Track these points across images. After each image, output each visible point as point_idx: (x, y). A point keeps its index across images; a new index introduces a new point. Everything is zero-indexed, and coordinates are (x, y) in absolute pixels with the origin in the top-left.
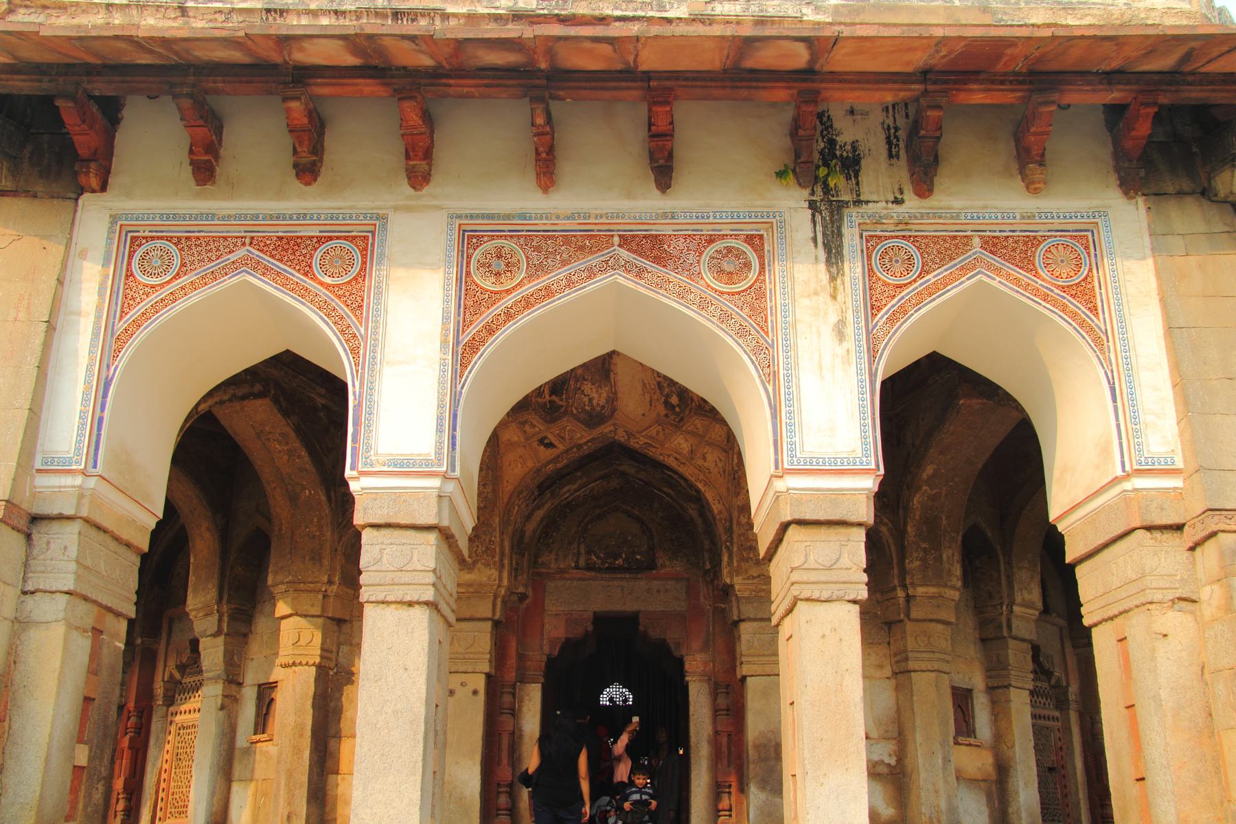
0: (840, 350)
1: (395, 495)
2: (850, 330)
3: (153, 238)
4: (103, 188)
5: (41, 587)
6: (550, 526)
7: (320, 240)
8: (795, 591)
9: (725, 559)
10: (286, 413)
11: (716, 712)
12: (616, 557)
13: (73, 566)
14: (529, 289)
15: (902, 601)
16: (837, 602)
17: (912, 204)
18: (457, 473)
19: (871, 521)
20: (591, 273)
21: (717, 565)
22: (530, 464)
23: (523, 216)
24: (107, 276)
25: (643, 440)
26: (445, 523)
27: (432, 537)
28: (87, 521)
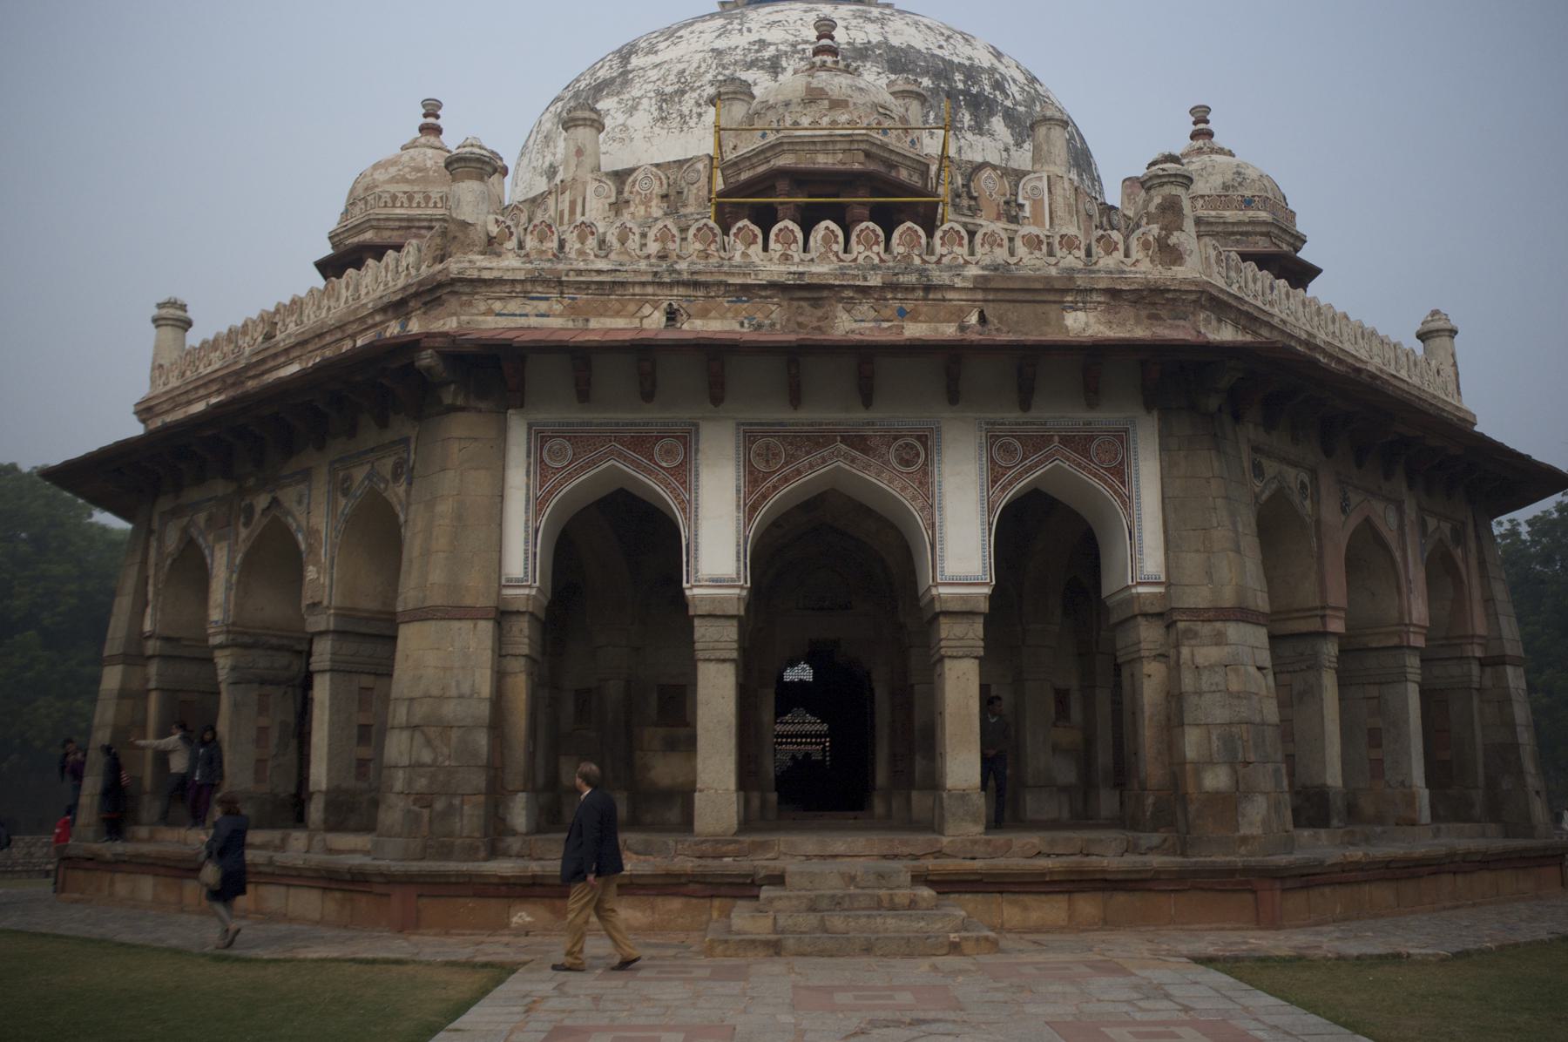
1: (713, 599)
4: (522, 406)
5: (510, 652)
7: (658, 438)
8: (943, 652)
13: (526, 640)
14: (787, 470)
16: (965, 660)
17: (1014, 415)
18: (749, 585)
19: (987, 611)
20: (824, 461)
23: (781, 424)
24: (529, 464)
28: (532, 614)
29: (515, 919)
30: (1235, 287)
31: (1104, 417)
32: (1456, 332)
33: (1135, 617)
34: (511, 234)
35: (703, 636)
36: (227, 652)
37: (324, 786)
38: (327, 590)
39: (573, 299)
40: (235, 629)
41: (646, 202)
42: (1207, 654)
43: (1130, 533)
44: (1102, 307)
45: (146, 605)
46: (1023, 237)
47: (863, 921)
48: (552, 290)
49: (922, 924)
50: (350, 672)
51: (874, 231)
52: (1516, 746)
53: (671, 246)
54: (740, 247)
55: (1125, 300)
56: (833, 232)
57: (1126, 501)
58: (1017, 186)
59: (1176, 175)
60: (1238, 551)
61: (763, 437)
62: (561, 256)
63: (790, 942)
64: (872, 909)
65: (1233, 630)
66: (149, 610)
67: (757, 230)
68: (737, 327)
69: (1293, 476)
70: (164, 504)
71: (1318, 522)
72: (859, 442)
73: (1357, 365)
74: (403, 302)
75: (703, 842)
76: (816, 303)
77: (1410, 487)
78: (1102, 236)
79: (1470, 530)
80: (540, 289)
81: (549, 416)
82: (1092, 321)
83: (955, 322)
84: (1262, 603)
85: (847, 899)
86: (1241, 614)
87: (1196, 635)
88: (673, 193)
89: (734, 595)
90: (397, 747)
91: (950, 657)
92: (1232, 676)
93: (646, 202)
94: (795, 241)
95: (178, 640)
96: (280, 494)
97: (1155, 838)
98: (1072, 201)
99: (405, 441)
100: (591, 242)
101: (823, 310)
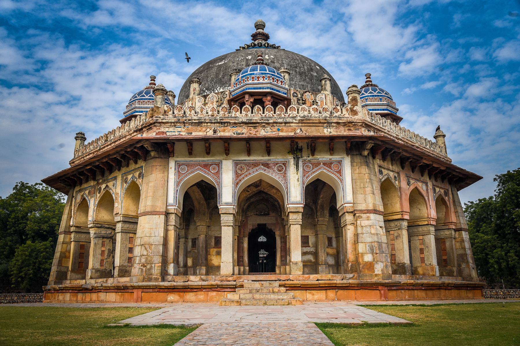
0: (298, 183)
1: (226, 209)
2: (300, 180)
3: (182, 165)
4: (173, 157)
6: (249, 206)
7: (211, 165)
8: (290, 223)
9: (283, 213)
10: (198, 188)
11: (281, 242)
12: (262, 212)
13: (174, 221)
15: (317, 221)
17: (311, 157)
18: (236, 205)
19: (303, 211)
21: (281, 214)
22: (245, 195)
23: (245, 161)
25: (266, 190)
26: (234, 213)
27: (232, 215)
29: (169, 299)
30: (374, 121)
31: (335, 158)
32: (445, 136)
33: (345, 213)
34: (171, 110)
35: (223, 219)
36: (93, 229)
37: (118, 265)
38: (120, 209)
40: (95, 222)
41: (212, 103)
42: (365, 223)
43: (343, 189)
44: (335, 127)
45: (71, 217)
46: (313, 108)
47: (264, 296)
48: (182, 125)
49: (281, 296)
50: (127, 233)
51: (271, 108)
52: (466, 255)
53: (215, 112)
54: (234, 112)
56: (259, 108)
57: (342, 181)
58: (316, 97)
59: (355, 91)
60: (374, 194)
61: (240, 164)
62: (185, 115)
63: (243, 302)
64: (267, 293)
65: (372, 216)
66: (72, 219)
67: (239, 108)
68: (233, 134)
69: (391, 174)
70: (77, 188)
71: (400, 188)
72: (266, 165)
74: (142, 129)
75: (222, 277)
76: (255, 127)
77: (430, 179)
78: (335, 108)
79: (450, 192)
80: (178, 125)
81: (180, 159)
83: (293, 132)
84: (381, 209)
85: (260, 290)
86: (375, 211)
87: (361, 217)
88: (219, 100)
89: (232, 209)
90: (137, 251)
91: (292, 224)
93: (212, 103)
94: (249, 110)
95: (80, 227)
96: (108, 184)
97: (351, 275)
98: (332, 101)
99: (142, 167)
100: (193, 112)
101: (257, 129)
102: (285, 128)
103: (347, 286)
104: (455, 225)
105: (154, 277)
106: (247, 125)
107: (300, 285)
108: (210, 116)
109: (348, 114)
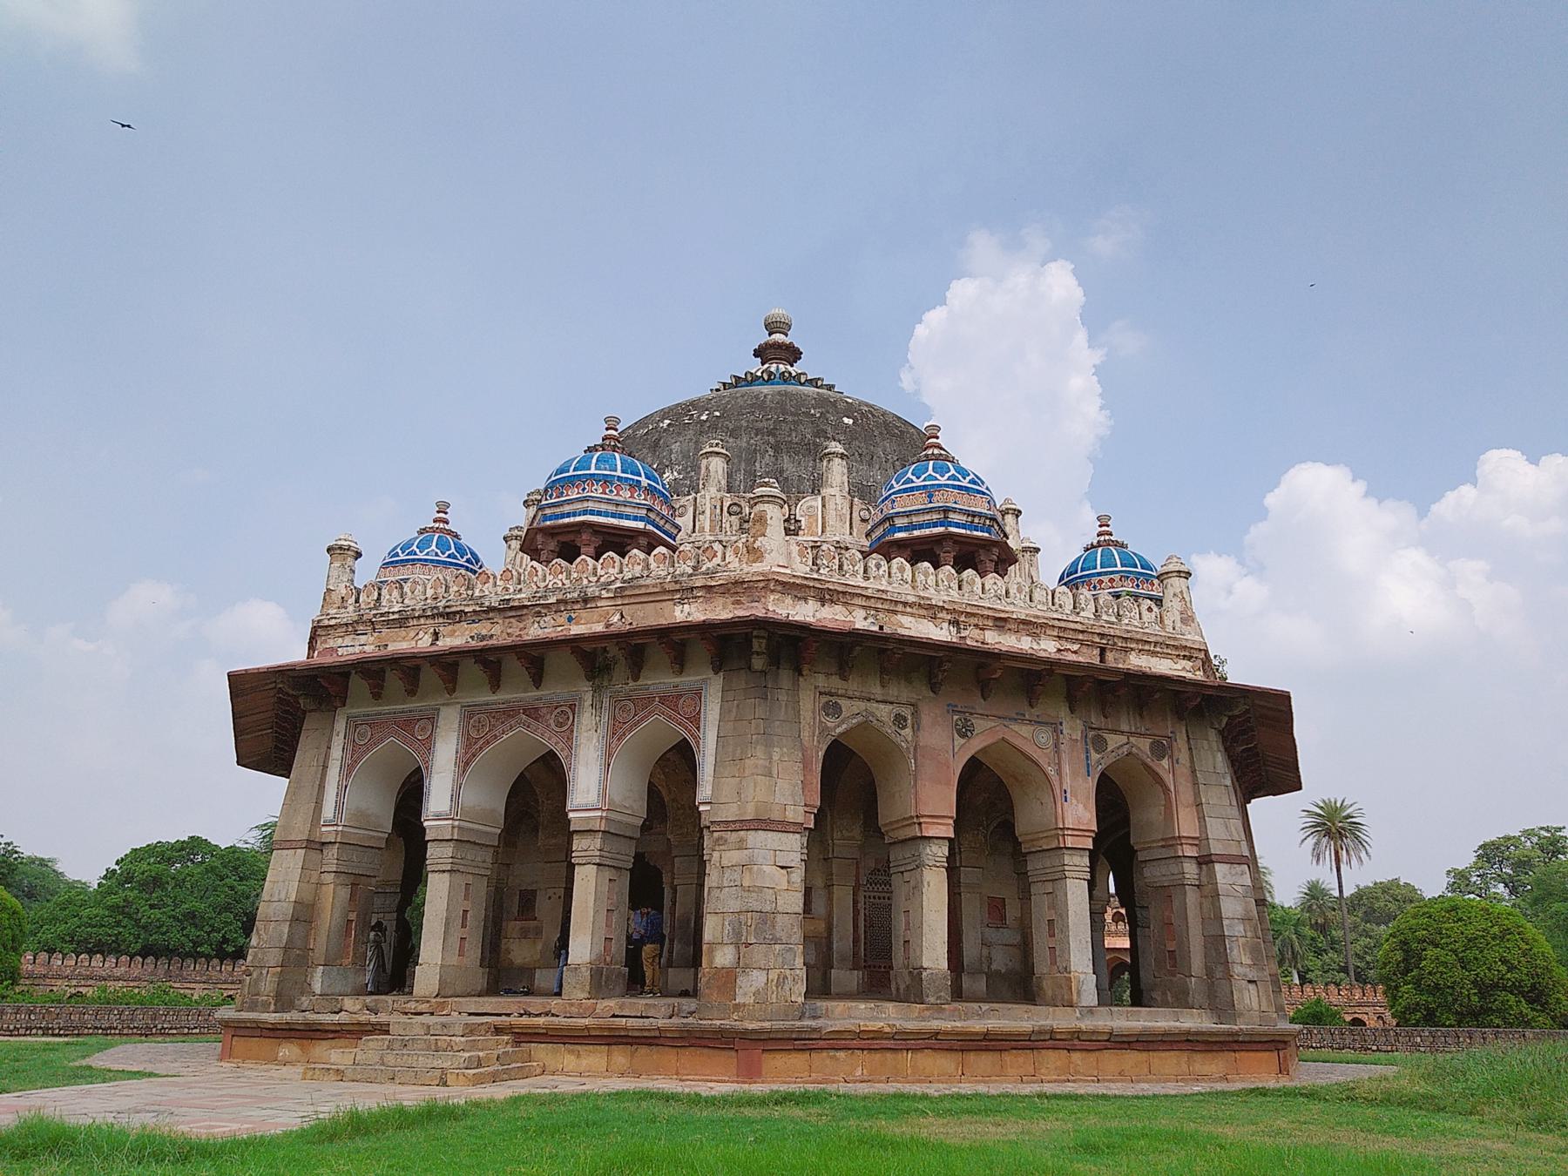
31: (687, 680)
39: (380, 632)
44: (701, 600)
53: (439, 590)
55: (716, 593)
56: (535, 569)
59: (762, 496)
68: (470, 640)
72: (533, 712)
73: (997, 615)
76: (520, 618)
79: (1181, 742)
82: (693, 610)
83: (602, 622)
91: (577, 864)
92: (747, 875)
102: (583, 613)
103: (655, 1037)
104: (1196, 845)
105: (260, 999)
106: (503, 614)
107: (544, 1031)
108: (429, 601)
109: (737, 559)
